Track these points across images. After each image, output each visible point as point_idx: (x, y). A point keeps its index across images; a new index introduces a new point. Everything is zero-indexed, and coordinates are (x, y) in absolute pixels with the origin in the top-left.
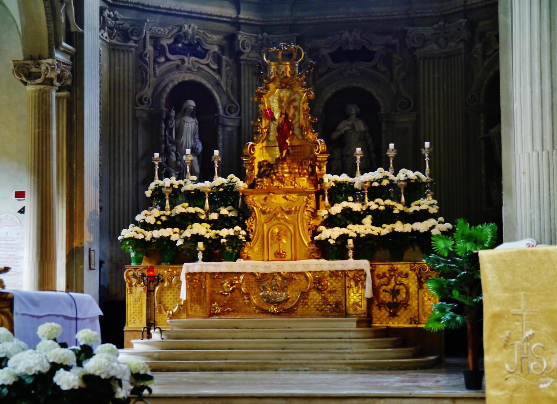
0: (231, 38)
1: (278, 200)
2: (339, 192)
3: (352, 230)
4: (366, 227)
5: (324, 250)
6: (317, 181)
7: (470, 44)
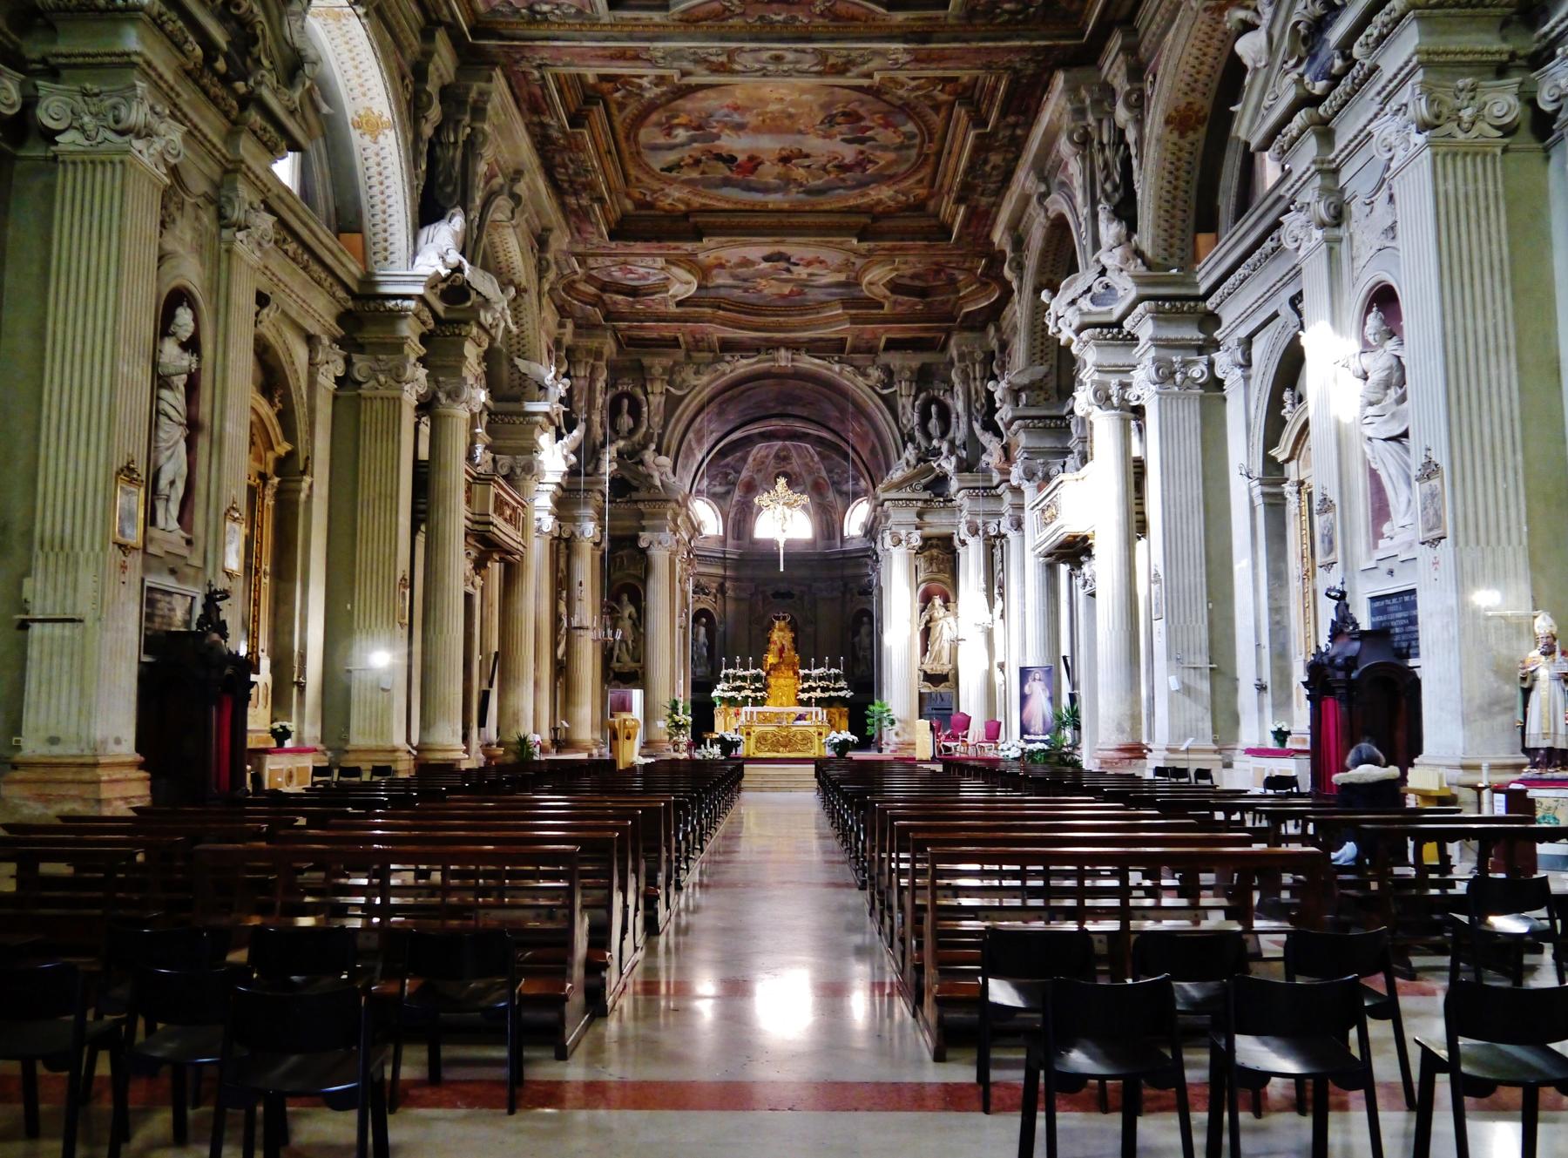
0: (722, 586)
1: (782, 681)
2: (806, 678)
3: (812, 694)
4: (818, 694)
5: (801, 703)
6: (796, 673)
7: (844, 593)
